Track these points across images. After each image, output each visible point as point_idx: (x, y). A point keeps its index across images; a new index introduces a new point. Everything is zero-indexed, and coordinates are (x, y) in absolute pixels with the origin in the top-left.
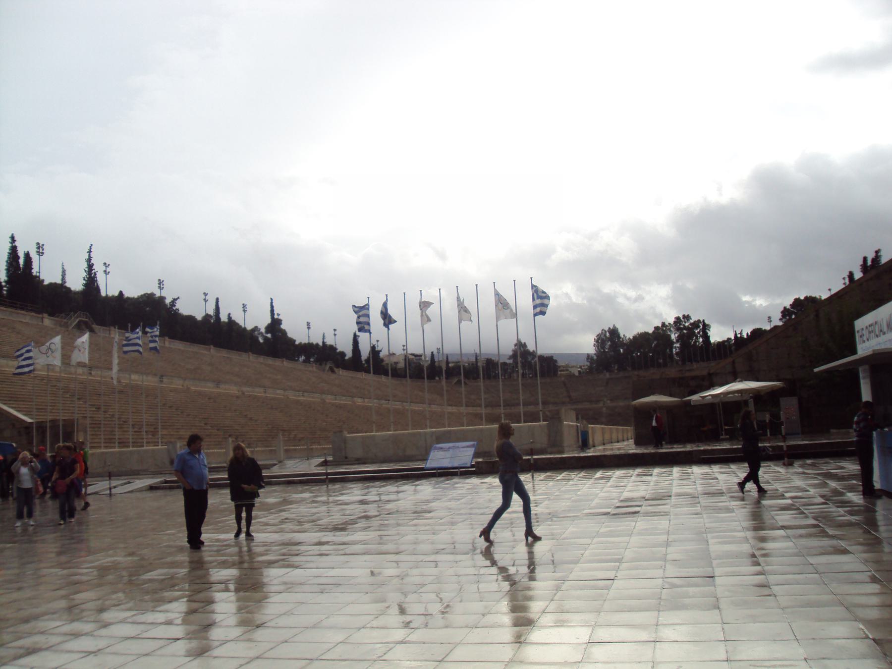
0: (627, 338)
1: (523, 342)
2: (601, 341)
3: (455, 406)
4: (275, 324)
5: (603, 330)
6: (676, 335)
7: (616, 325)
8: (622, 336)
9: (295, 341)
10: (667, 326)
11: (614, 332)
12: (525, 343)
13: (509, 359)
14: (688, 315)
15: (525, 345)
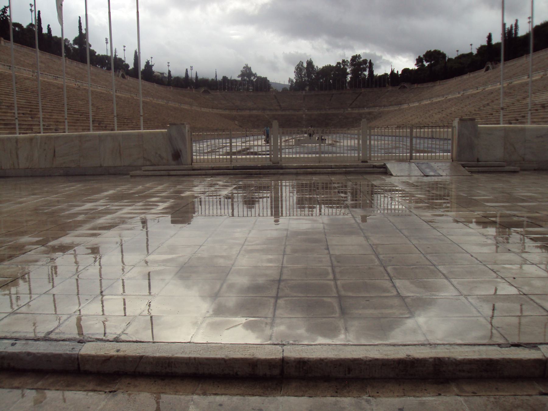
0: (319, 68)
1: (249, 66)
2: (299, 69)
3: (206, 108)
4: (82, 39)
5: (301, 62)
6: (350, 69)
7: (312, 59)
8: (315, 67)
9: (96, 52)
10: (346, 62)
11: (310, 63)
12: (250, 68)
13: (239, 77)
14: (359, 55)
15: (250, 69)
